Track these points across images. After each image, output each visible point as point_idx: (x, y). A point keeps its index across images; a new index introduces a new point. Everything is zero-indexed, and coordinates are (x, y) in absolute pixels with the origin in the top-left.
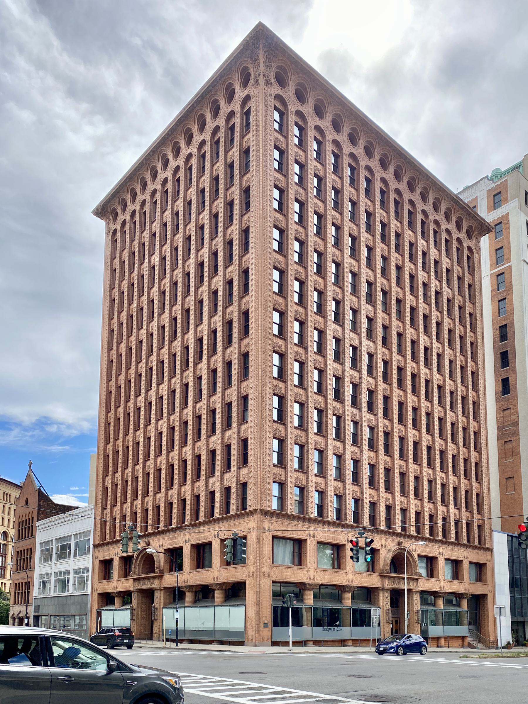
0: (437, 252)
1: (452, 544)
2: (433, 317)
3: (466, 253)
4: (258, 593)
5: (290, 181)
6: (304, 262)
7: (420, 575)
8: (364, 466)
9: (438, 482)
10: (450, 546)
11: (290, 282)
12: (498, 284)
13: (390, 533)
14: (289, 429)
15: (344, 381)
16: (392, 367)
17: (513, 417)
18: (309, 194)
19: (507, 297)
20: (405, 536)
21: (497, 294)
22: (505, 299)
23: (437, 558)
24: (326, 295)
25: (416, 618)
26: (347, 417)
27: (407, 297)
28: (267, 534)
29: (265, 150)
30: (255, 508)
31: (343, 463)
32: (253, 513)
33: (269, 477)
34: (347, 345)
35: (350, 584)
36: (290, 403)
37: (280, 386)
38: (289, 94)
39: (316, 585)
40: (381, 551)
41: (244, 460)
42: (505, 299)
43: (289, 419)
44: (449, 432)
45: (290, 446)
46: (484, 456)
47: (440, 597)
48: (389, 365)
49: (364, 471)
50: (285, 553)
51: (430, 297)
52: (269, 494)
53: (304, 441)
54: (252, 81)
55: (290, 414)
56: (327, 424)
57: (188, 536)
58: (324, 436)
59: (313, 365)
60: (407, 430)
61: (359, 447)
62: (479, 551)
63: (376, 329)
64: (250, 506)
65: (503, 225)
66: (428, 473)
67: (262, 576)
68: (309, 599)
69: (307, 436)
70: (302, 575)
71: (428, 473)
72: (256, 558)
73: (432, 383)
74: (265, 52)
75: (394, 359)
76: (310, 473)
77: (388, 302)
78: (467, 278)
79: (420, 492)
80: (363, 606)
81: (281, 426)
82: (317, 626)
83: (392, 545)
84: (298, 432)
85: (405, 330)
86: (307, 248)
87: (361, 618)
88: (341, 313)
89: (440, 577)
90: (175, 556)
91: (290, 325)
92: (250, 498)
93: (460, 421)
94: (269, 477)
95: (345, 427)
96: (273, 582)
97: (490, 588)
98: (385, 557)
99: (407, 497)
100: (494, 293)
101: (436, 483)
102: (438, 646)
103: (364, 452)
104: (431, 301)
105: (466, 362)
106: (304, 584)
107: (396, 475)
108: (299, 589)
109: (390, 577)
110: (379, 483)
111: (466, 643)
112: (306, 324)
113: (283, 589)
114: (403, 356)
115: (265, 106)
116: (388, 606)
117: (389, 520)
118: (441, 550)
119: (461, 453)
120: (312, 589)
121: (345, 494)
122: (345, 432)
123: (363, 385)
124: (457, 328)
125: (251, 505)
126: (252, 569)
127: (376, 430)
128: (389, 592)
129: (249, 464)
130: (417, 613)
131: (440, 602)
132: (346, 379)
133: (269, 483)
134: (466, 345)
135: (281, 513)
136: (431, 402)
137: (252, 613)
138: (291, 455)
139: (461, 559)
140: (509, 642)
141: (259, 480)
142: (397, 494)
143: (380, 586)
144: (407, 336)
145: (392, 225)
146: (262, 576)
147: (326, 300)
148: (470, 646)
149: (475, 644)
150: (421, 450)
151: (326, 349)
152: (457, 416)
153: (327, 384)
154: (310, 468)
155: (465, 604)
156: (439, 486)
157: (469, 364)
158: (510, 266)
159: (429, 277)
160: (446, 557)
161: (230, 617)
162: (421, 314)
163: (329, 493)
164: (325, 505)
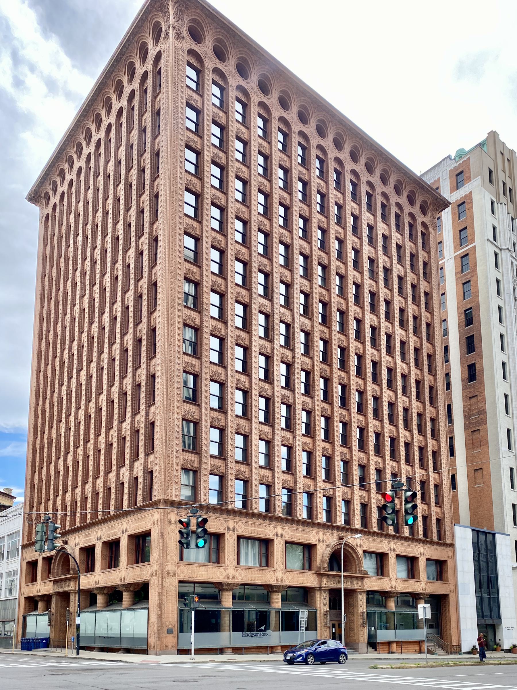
1: (405, 539)
2: (381, 295)
3: (420, 229)
4: (161, 594)
5: (206, 142)
6: (225, 230)
7: (366, 572)
10: (403, 542)
11: (205, 250)
12: (462, 266)
14: (204, 411)
15: (273, 360)
16: (332, 347)
17: (480, 405)
19: (472, 279)
20: (347, 530)
21: (462, 277)
22: (469, 281)
24: (251, 267)
25: (361, 621)
28: (173, 526)
29: (175, 108)
30: (159, 498)
32: (157, 504)
33: (177, 464)
34: (276, 321)
35: (279, 583)
36: (204, 381)
37: (194, 363)
40: (318, 547)
42: (469, 281)
43: (204, 399)
44: (401, 418)
45: (204, 429)
47: (391, 597)
48: (328, 345)
49: (297, 458)
51: (378, 273)
52: (176, 483)
55: (204, 393)
56: (251, 406)
58: (249, 420)
61: (292, 432)
62: (438, 547)
63: (312, 305)
64: (155, 496)
65: (466, 204)
67: (165, 575)
68: (227, 601)
70: (218, 574)
72: (158, 555)
73: (381, 365)
75: (333, 337)
76: (229, 460)
77: (327, 277)
80: (294, 608)
81: (194, 407)
83: (331, 540)
85: (347, 307)
87: (290, 622)
88: (270, 286)
89: (391, 576)
91: (205, 295)
93: (413, 406)
95: (274, 410)
96: (180, 582)
98: (323, 553)
100: (459, 276)
101: (385, 473)
102: (390, 652)
103: (298, 437)
104: (378, 278)
105: (421, 344)
106: (220, 583)
108: (213, 591)
109: (328, 575)
110: (316, 471)
112: (226, 297)
114: (346, 336)
116: (327, 608)
117: (330, 512)
118: (392, 545)
119: (415, 440)
120: (231, 590)
122: (274, 415)
123: (296, 365)
124: (409, 307)
125: (158, 495)
126: (155, 568)
127: (313, 414)
128: (327, 592)
129: (155, 449)
131: (392, 603)
132: (276, 357)
134: (421, 325)
136: (379, 385)
137: (154, 618)
138: (206, 439)
139: (417, 555)
140: (474, 647)
143: (317, 585)
146: (165, 575)
147: (251, 272)
148: (429, 652)
151: (251, 325)
152: (410, 401)
153: (251, 362)
154: (230, 454)
157: (424, 346)
158: (475, 247)
159: (377, 252)
160: (398, 553)
161: (132, 622)
163: (254, 482)
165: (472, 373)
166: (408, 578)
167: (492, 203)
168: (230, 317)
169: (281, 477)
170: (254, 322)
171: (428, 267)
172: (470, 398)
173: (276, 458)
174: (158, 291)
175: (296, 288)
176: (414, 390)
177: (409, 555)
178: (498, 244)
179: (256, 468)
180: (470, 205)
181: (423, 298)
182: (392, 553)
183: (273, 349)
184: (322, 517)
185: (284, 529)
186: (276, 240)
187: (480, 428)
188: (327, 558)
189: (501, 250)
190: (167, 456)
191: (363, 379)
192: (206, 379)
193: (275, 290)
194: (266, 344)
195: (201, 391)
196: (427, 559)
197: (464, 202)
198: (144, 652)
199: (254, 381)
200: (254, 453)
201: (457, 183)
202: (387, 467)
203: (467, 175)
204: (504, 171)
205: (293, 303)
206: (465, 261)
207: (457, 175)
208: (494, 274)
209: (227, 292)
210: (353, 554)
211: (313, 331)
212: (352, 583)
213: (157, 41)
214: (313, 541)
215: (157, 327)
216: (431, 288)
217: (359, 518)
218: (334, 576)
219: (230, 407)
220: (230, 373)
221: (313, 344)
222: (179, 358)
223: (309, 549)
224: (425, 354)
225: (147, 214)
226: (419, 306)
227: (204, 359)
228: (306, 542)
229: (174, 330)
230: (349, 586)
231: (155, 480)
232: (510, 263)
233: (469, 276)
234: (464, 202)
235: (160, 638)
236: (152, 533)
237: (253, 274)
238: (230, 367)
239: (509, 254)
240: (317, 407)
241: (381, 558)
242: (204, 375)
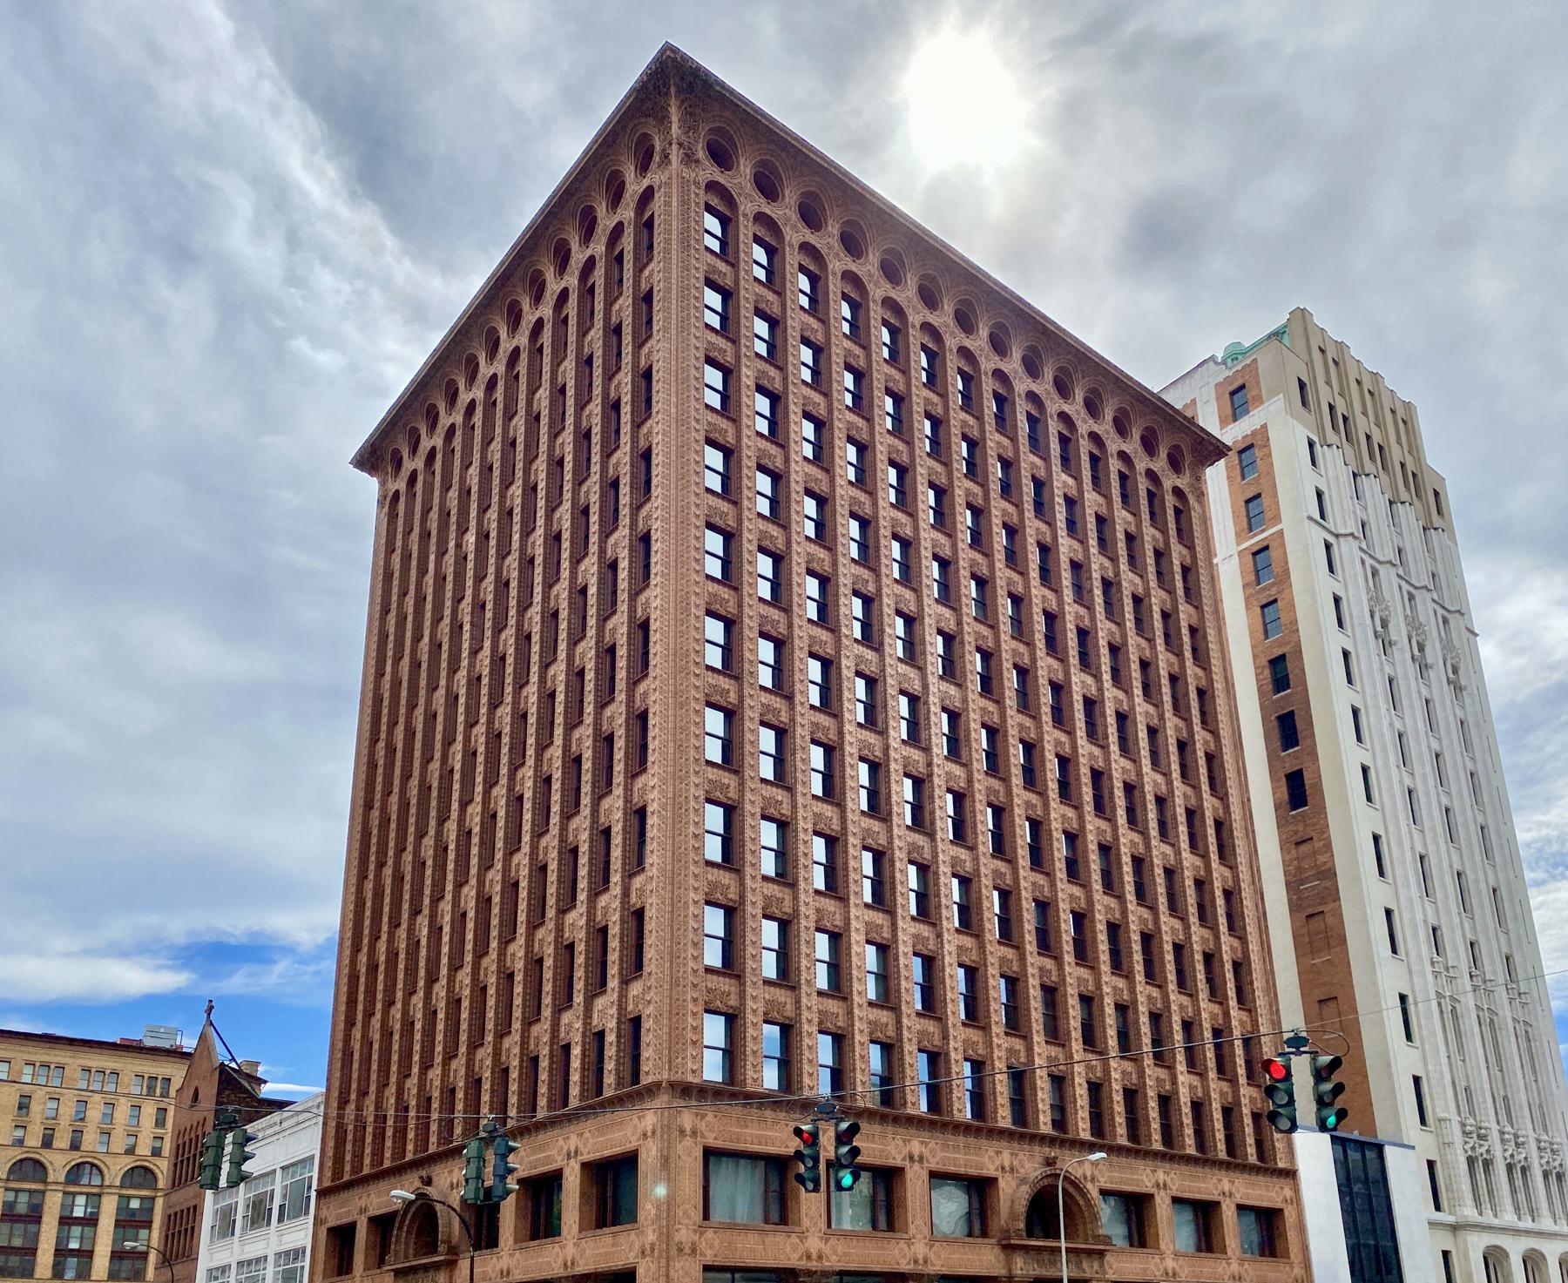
0: (1100, 499)
1: (1188, 1160)
3: (1170, 501)
7: (1107, 1240)
8: (948, 970)
9: (1143, 1009)
12: (1257, 572)
13: (1022, 1136)
14: (748, 882)
15: (888, 771)
17: (1321, 859)
20: (1063, 1143)
22: (1275, 601)
23: (1151, 1197)
26: (897, 853)
27: (1034, 592)
28: (688, 1142)
32: (652, 1090)
33: (695, 1000)
36: (749, 821)
37: (726, 781)
38: (741, 180)
40: (1002, 1183)
42: (1275, 601)
43: (748, 857)
44: (1161, 890)
45: (750, 923)
46: (1254, 946)
48: (999, 737)
50: (739, 1193)
51: (1091, 591)
52: (694, 1043)
53: (790, 911)
54: (657, 158)
55: (749, 846)
59: (806, 733)
60: (1053, 885)
61: (934, 925)
63: (963, 657)
65: (1257, 452)
66: (1115, 988)
69: (795, 898)
71: (1115, 988)
74: (683, 101)
75: (1010, 721)
81: (727, 875)
83: (1028, 1165)
85: (1034, 660)
88: (875, 622)
89: (1163, 1247)
91: (747, 645)
92: (647, 1053)
94: (695, 1000)
95: (893, 877)
96: (707, 1268)
98: (1012, 1196)
99: (1064, 1046)
100: (1251, 591)
101: (1136, 1011)
104: (1093, 600)
105: (1191, 733)
107: (1031, 991)
109: (1026, 1249)
115: (684, 203)
118: (1161, 1176)
119: (1194, 938)
121: (900, 1040)
122: (893, 888)
123: (936, 781)
125: (652, 1069)
126: (651, 1237)
127: (974, 885)
132: (893, 766)
133: (694, 1014)
134: (1187, 694)
139: (1216, 1198)
142: (1038, 1038)
143: (1004, 1272)
144: (1040, 672)
146: (674, 1252)
147: (837, 595)
150: (1094, 931)
152: (1178, 853)
156: (1144, 1019)
158: (1281, 532)
159: (1086, 550)
162: (1071, 626)
163: (858, 1037)
164: (848, 1067)
165: (1297, 791)
166: (1199, 1250)
167: (1311, 445)
168: (798, 686)
169: (913, 1026)
170: (846, 694)
171: (1191, 577)
173: (903, 984)
174: (652, 639)
175: (929, 623)
176: (1183, 829)
177: (1198, 1196)
178: (1331, 526)
179: (860, 1006)
181: (1186, 639)
182: (1162, 1193)
183: (886, 748)
184: (1003, 1117)
185: (927, 1144)
186: (885, 532)
188: (1022, 1207)
189: (1337, 536)
190: (675, 983)
191: (1076, 808)
192: (753, 815)
193: (887, 629)
194: (871, 738)
195: (743, 840)
199: (850, 815)
200: (855, 973)
201: (1234, 410)
202: (1141, 999)
205: (924, 653)
207: (1233, 393)
208: (1326, 586)
209: (791, 636)
210: (1078, 1198)
211: (966, 710)
212: (1079, 1265)
214: (990, 1170)
215: (651, 711)
216: (1202, 618)
217: (1086, 1115)
218: (1039, 1249)
219: (802, 873)
220: (800, 800)
221: (968, 736)
222: (697, 773)
223: (979, 1189)
224: (1200, 754)
225: (625, 490)
226: (1179, 654)
227: (748, 772)
228: (972, 1171)
229: (688, 716)
230: (1075, 1274)
231: (645, 1038)
233: (1274, 591)
234: (1252, 446)
236: (642, 1157)
237: (842, 600)
238: (800, 788)
239: (1355, 544)
240: (983, 870)
241: (1136, 1207)
242: (748, 807)
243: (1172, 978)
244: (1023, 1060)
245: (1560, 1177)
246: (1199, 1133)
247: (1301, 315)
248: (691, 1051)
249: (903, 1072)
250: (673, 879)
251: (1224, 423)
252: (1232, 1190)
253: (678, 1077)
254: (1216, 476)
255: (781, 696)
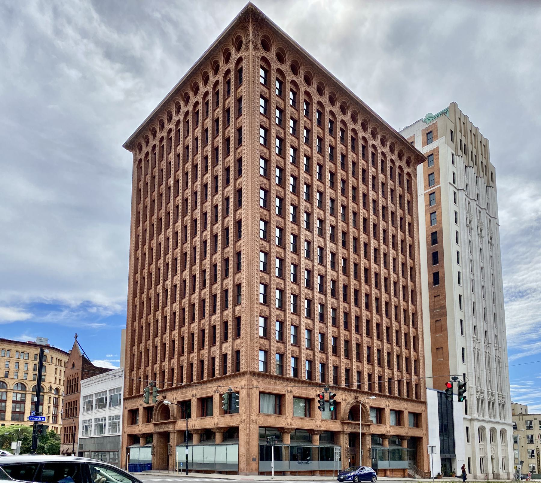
0: (384, 177)
1: (395, 398)
2: (381, 226)
3: (406, 177)
4: (248, 435)
5: (272, 122)
9: (385, 351)
11: (272, 199)
12: (430, 201)
13: (348, 390)
14: (272, 310)
17: (442, 302)
18: (287, 133)
19: (437, 211)
22: (435, 212)
25: (368, 454)
27: (361, 211)
28: (255, 389)
30: (246, 370)
31: (313, 336)
32: (244, 374)
33: (257, 346)
34: (315, 246)
35: (318, 429)
36: (272, 290)
37: (265, 277)
39: (292, 429)
40: (342, 404)
41: (238, 334)
42: (435, 212)
43: (272, 302)
44: (393, 313)
47: (387, 438)
50: (269, 405)
51: (378, 210)
52: (257, 360)
55: (272, 298)
56: (300, 306)
57: (195, 392)
58: (299, 315)
59: (289, 261)
60: (361, 311)
61: (325, 324)
65: (434, 157)
66: (377, 344)
67: (251, 422)
68: (287, 440)
69: (285, 315)
71: (377, 344)
72: (246, 409)
73: (380, 275)
75: (351, 257)
76: (288, 343)
78: (407, 196)
79: (372, 358)
82: (294, 460)
83: (350, 399)
84: (279, 312)
86: (285, 173)
87: (327, 455)
88: (311, 222)
90: (185, 407)
91: (272, 231)
92: (242, 362)
93: (401, 304)
94: (257, 346)
95: (314, 308)
96: (260, 427)
97: (424, 432)
98: (345, 408)
100: (427, 208)
101: (383, 352)
102: (385, 476)
103: (329, 327)
104: (379, 214)
105: (406, 260)
106: (283, 428)
108: (279, 432)
109: (348, 423)
111: (406, 474)
113: (267, 433)
116: (347, 446)
118: (387, 403)
119: (402, 329)
120: (290, 432)
122: (314, 312)
123: (328, 277)
125: (243, 367)
126: (244, 417)
127: (338, 311)
128: (348, 435)
129: (242, 336)
130: (369, 451)
131: (387, 442)
132: (315, 272)
133: (257, 351)
134: (406, 247)
135: (266, 375)
137: (243, 450)
139: (403, 410)
140: (439, 474)
141: (249, 349)
143: (341, 430)
144: (361, 239)
145: (349, 156)
146: (251, 422)
147: (300, 212)
148: (410, 476)
149: (413, 474)
150: (372, 326)
151: (300, 249)
152: (399, 301)
155: (405, 444)
157: (408, 262)
159: (378, 195)
160: (391, 408)
162: (371, 223)
163: (303, 359)
164: (299, 368)
165: (436, 279)
167: (453, 155)
171: (410, 205)
172: (435, 297)
178: (456, 186)
180: (437, 157)
187: (442, 319)
189: (458, 190)
196: (409, 413)
197: (433, 154)
198: (236, 473)
201: (428, 140)
203: (435, 134)
204: (460, 131)
206: (433, 197)
207: (427, 134)
208: (453, 208)
213: (238, 49)
218: (351, 424)
224: (409, 267)
232: (464, 199)
233: (435, 209)
235: (248, 464)
241: (380, 412)
243: (395, 341)
244: (349, 366)
245: (504, 405)
246: (399, 390)
247: (454, 105)
248: (256, 362)
249: (315, 369)
250: (250, 308)
251: (423, 145)
252: (406, 407)
253: (252, 370)
254: (420, 168)
255: (282, 248)
